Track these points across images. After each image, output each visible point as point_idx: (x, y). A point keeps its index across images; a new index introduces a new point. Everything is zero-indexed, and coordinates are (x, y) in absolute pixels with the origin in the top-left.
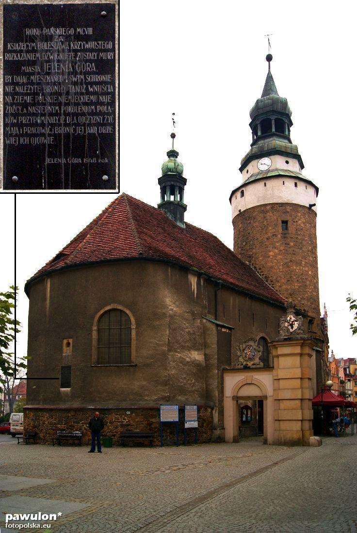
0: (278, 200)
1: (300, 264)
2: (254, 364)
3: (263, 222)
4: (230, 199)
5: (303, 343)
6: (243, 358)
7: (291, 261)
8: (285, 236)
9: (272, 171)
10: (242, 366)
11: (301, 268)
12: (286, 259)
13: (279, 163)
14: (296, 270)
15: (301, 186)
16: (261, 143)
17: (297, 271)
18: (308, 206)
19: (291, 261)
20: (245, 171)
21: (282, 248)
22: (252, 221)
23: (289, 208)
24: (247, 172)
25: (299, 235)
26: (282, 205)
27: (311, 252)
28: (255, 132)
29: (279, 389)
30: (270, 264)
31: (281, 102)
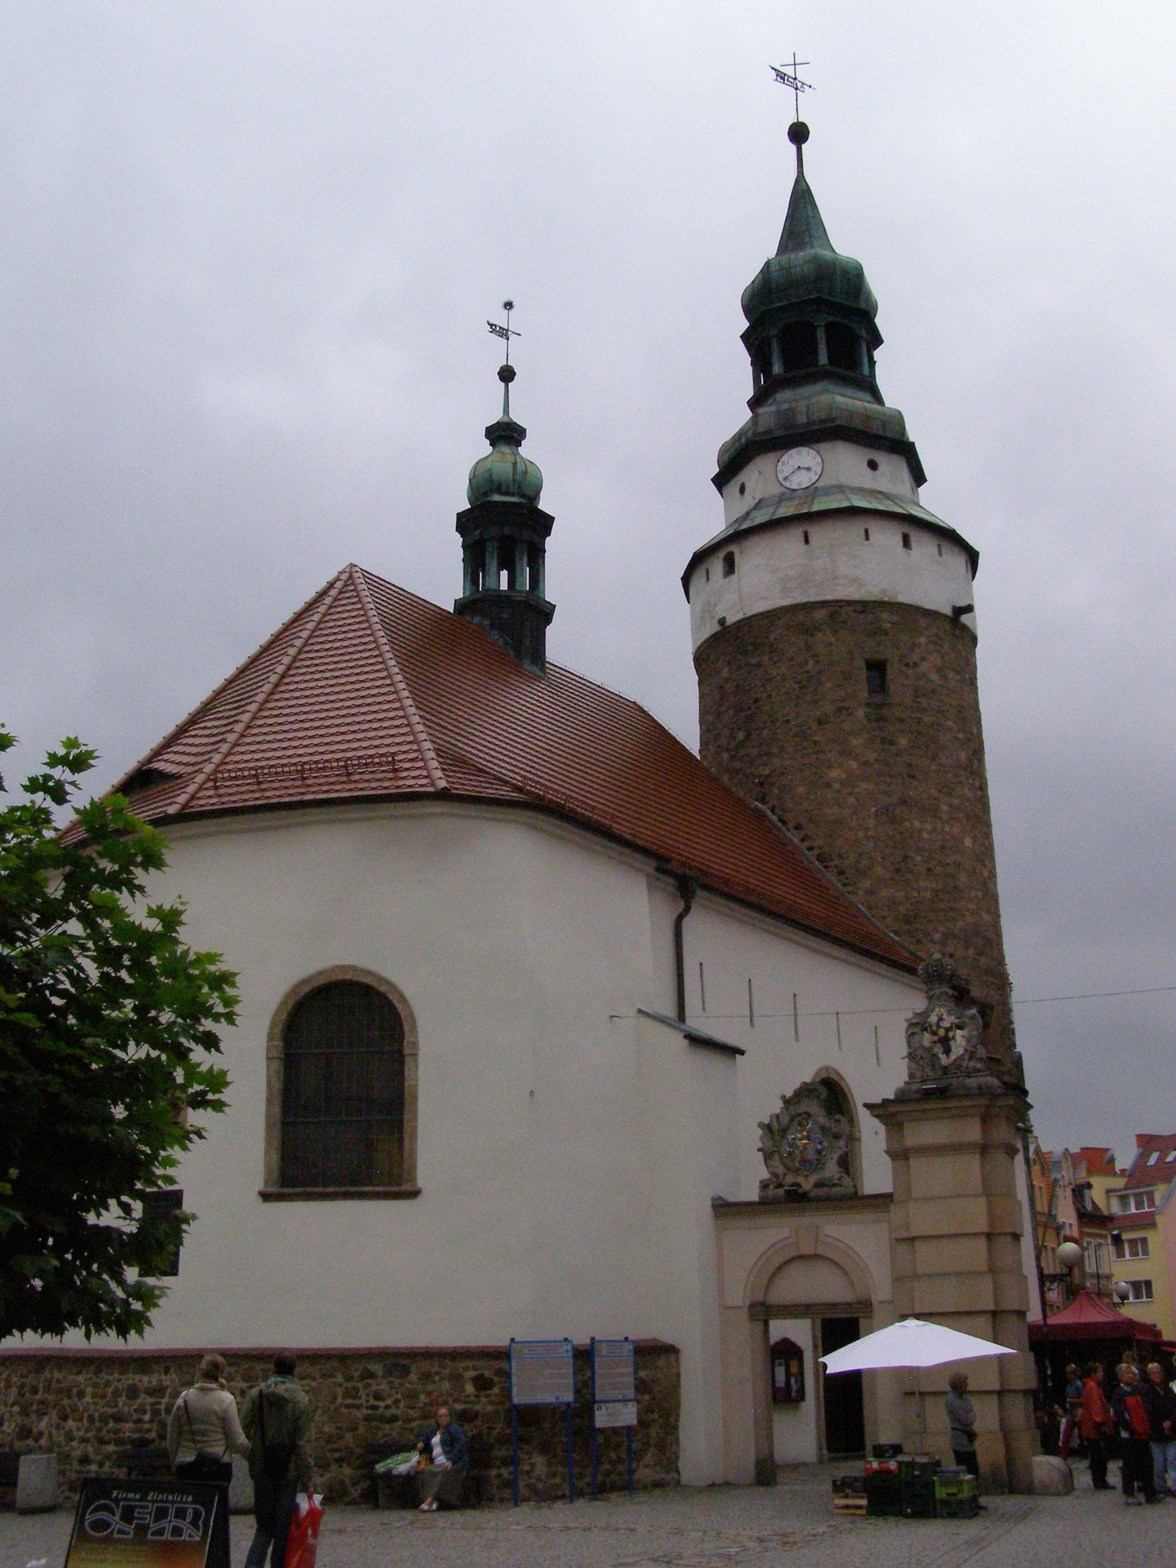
2: (819, 1185)
4: (686, 580)
5: (987, 1107)
6: (781, 1157)
7: (903, 802)
8: (879, 714)
9: (828, 491)
10: (781, 1191)
11: (939, 825)
12: (886, 793)
14: (920, 831)
15: (924, 547)
16: (784, 398)
18: (947, 611)
19: (903, 802)
20: (733, 487)
21: (872, 756)
26: (864, 607)
27: (965, 770)
28: (760, 362)
29: (916, 1276)
30: (831, 812)
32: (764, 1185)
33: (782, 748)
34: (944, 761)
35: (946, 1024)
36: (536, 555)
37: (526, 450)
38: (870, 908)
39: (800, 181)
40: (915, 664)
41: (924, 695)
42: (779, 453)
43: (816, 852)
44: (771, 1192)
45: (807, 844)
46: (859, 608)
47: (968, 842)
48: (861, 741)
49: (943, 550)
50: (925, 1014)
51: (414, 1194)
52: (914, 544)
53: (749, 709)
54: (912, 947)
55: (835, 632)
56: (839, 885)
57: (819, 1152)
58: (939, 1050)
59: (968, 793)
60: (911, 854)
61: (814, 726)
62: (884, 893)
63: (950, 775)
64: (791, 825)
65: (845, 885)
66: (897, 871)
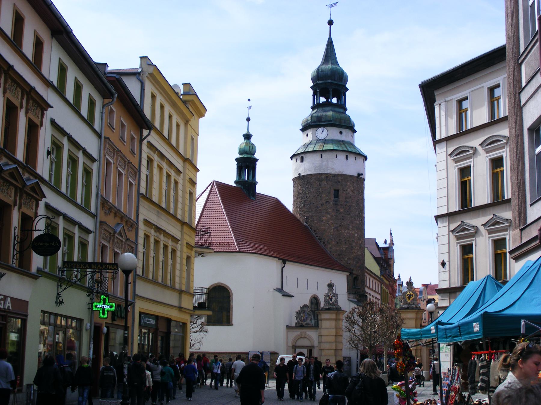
0: (332, 171)
1: (348, 229)
2: (306, 324)
7: (340, 226)
8: (336, 203)
10: (299, 325)
11: (349, 231)
12: (337, 224)
14: (344, 233)
15: (351, 158)
17: (345, 234)
18: (356, 175)
19: (340, 226)
21: (333, 214)
23: (340, 179)
24: (307, 135)
26: (335, 175)
27: (357, 216)
30: (323, 227)
31: (339, 73)
32: (296, 324)
33: (312, 210)
34: (351, 215)
35: (331, 295)
37: (253, 140)
38: (330, 252)
40: (346, 190)
41: (348, 198)
42: (317, 128)
43: (318, 237)
44: (297, 325)
45: (316, 235)
46: (333, 176)
47: (356, 235)
48: (331, 210)
49: (357, 158)
50: (328, 293)
52: (349, 158)
53: (305, 199)
54: (340, 262)
55: (327, 182)
56: (323, 246)
57: (306, 318)
58: (330, 300)
59: (358, 222)
60: (341, 239)
61: (320, 205)
62: (334, 248)
63: (353, 218)
64: (313, 230)
65: (325, 246)
66: (337, 243)
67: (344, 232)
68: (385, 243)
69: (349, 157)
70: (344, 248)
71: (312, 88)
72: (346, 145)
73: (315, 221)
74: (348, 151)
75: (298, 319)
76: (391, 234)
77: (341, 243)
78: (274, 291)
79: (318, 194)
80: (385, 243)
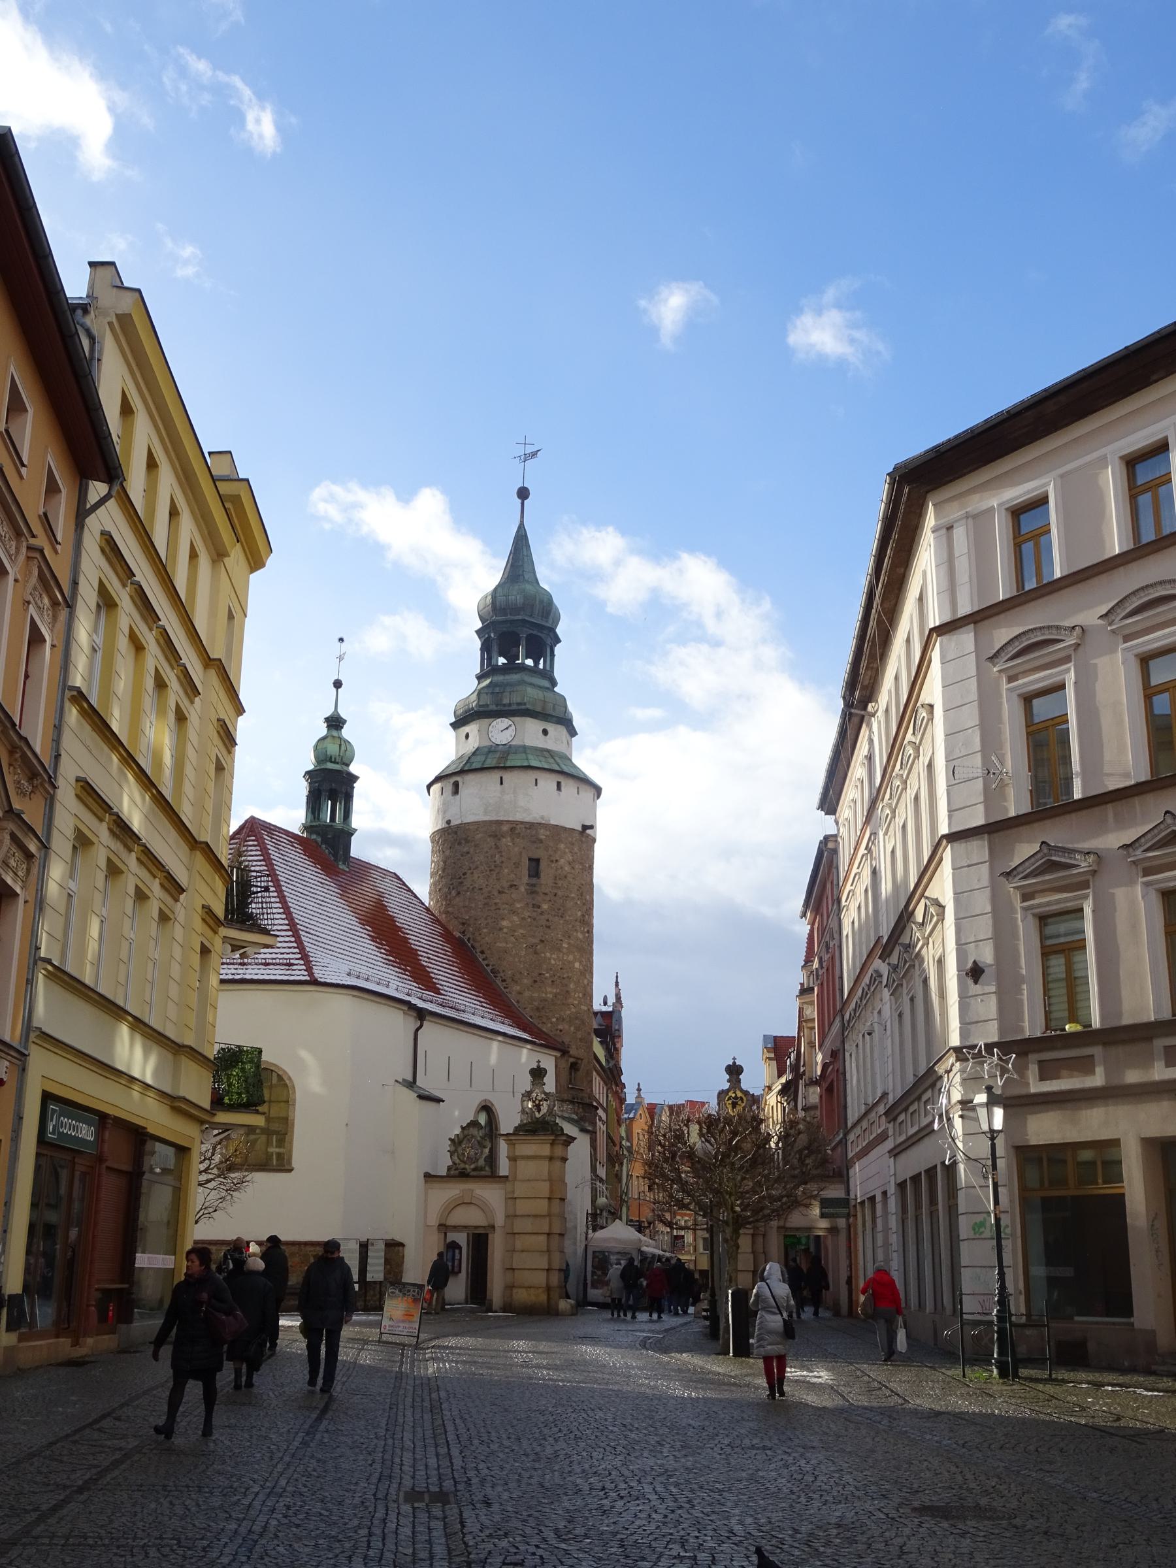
1: (559, 950)
3: (493, 856)
4: (429, 787)
5: (553, 1140)
7: (542, 941)
8: (532, 890)
10: (457, 1172)
13: (530, 733)
14: (550, 959)
15: (569, 787)
17: (553, 962)
18: (580, 829)
22: (472, 850)
23: (543, 834)
24: (467, 736)
25: (559, 888)
26: (531, 826)
29: (516, 1216)
31: (541, 602)
32: (449, 1168)
36: (348, 798)
37: (346, 732)
38: (518, 1002)
39: (521, 527)
40: (557, 861)
42: (491, 720)
43: (491, 967)
44: (452, 1172)
45: (486, 962)
47: (577, 965)
51: (290, 1170)
52: (562, 788)
54: (540, 1026)
59: (580, 936)
61: (496, 893)
66: (535, 981)
67: (552, 957)
68: (605, 1004)
69: (563, 784)
70: (551, 993)
71: (478, 632)
72: (557, 759)
73: (485, 930)
74: (562, 773)
75: (455, 1158)
76: (617, 984)
77: (543, 982)
78: (397, 1084)
79: (493, 867)
80: (605, 1004)
